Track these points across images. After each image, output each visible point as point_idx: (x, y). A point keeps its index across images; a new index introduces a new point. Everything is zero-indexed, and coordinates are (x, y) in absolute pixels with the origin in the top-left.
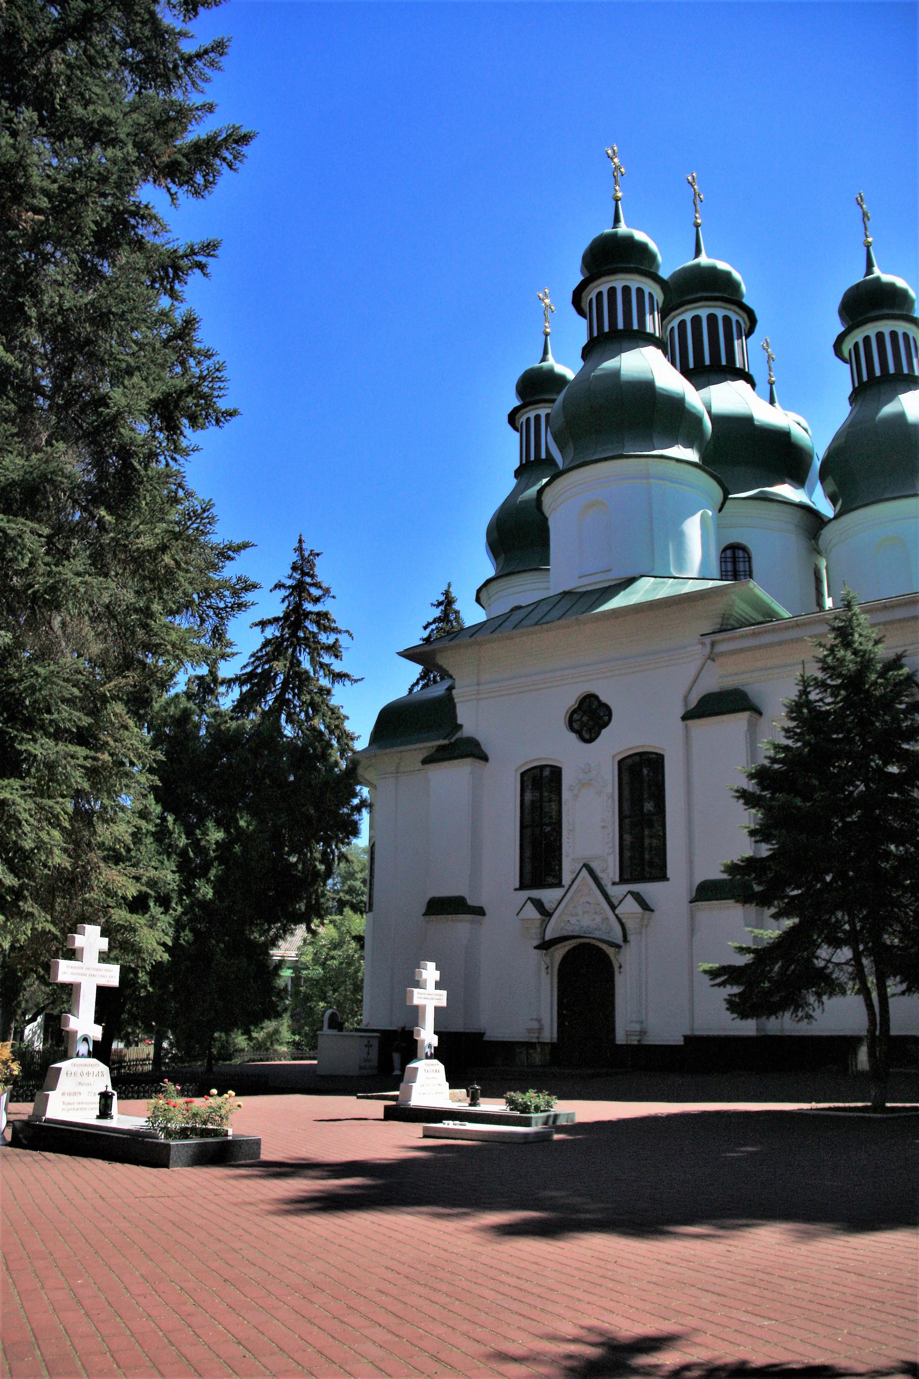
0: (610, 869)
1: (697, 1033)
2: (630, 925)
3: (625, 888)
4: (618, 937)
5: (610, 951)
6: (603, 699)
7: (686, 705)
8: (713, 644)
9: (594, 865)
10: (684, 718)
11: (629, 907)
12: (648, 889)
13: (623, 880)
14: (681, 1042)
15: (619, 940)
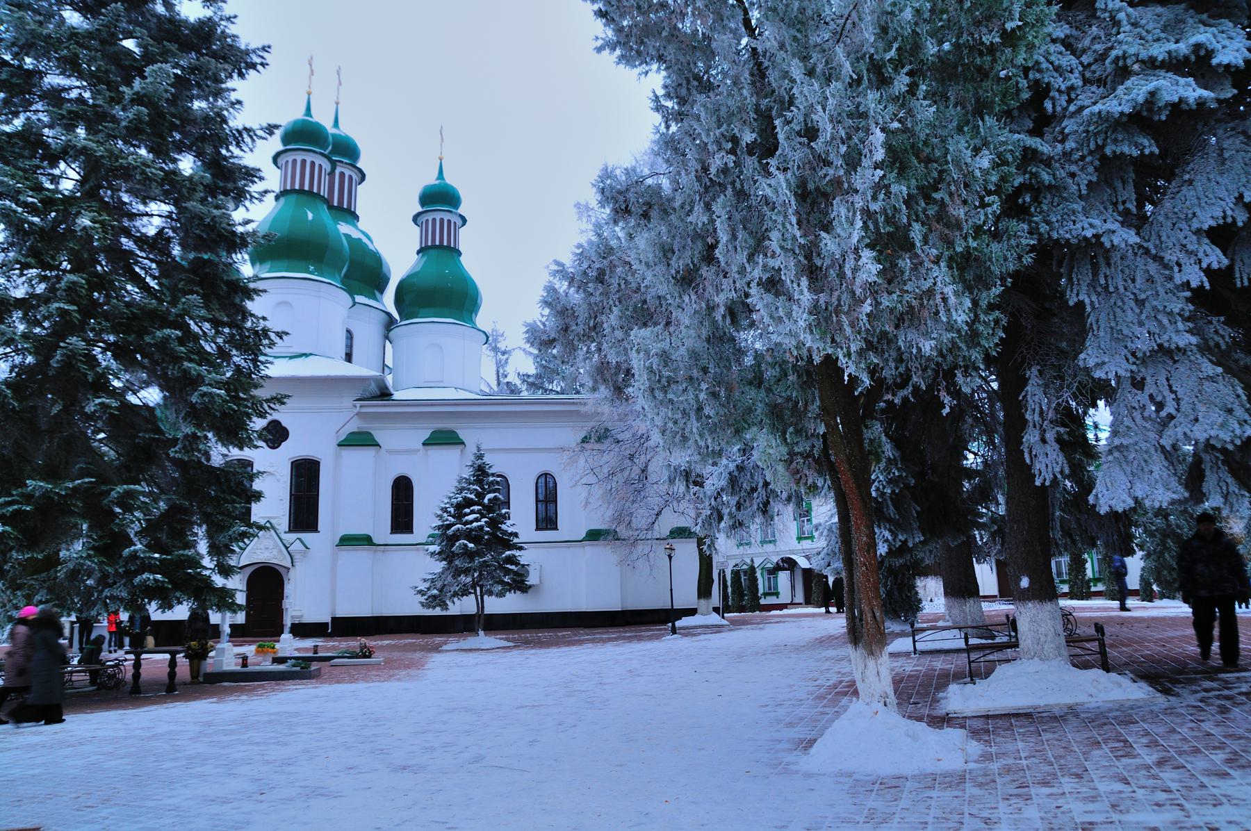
0: (283, 522)
1: (339, 614)
2: (296, 557)
3: (294, 536)
4: (288, 563)
5: (282, 571)
6: (284, 424)
7: (337, 437)
8: (361, 406)
9: (272, 521)
10: (339, 445)
11: (297, 546)
12: (307, 537)
13: (290, 531)
14: (329, 620)
15: (288, 564)
